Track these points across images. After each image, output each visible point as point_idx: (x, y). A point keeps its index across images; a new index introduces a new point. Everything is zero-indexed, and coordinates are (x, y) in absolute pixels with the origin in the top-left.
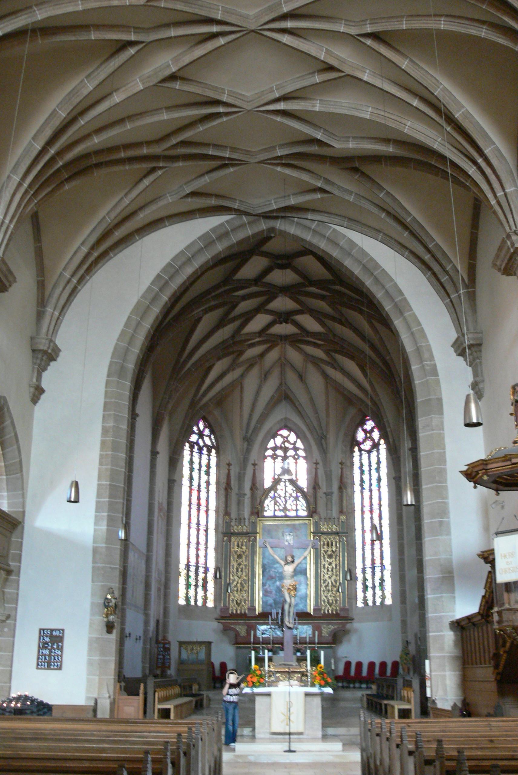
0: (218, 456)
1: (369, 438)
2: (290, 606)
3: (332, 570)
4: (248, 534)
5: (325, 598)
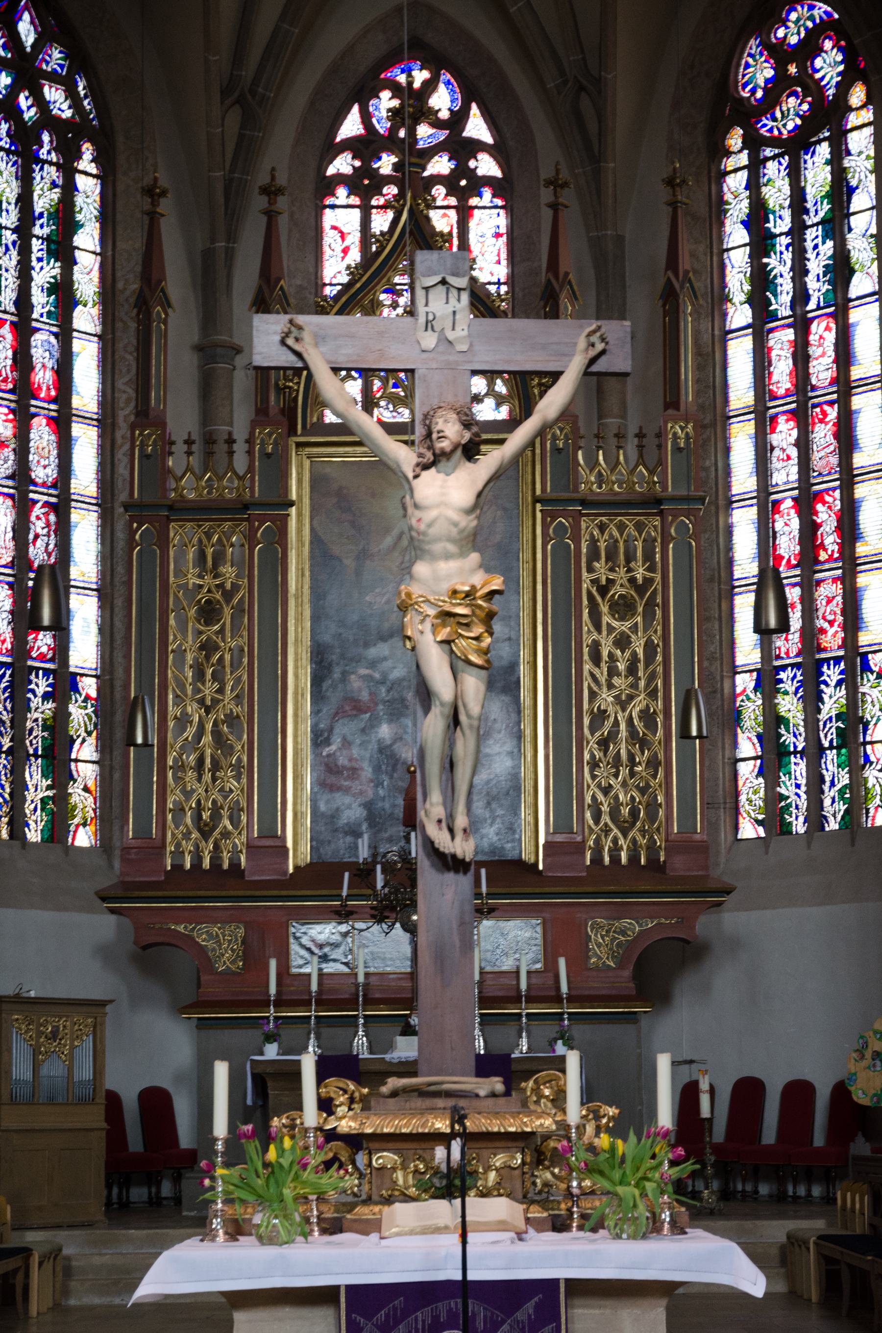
0: (105, 177)
1: (797, 80)
2: (455, 721)
3: (632, 670)
4: (246, 507)
5: (600, 797)
